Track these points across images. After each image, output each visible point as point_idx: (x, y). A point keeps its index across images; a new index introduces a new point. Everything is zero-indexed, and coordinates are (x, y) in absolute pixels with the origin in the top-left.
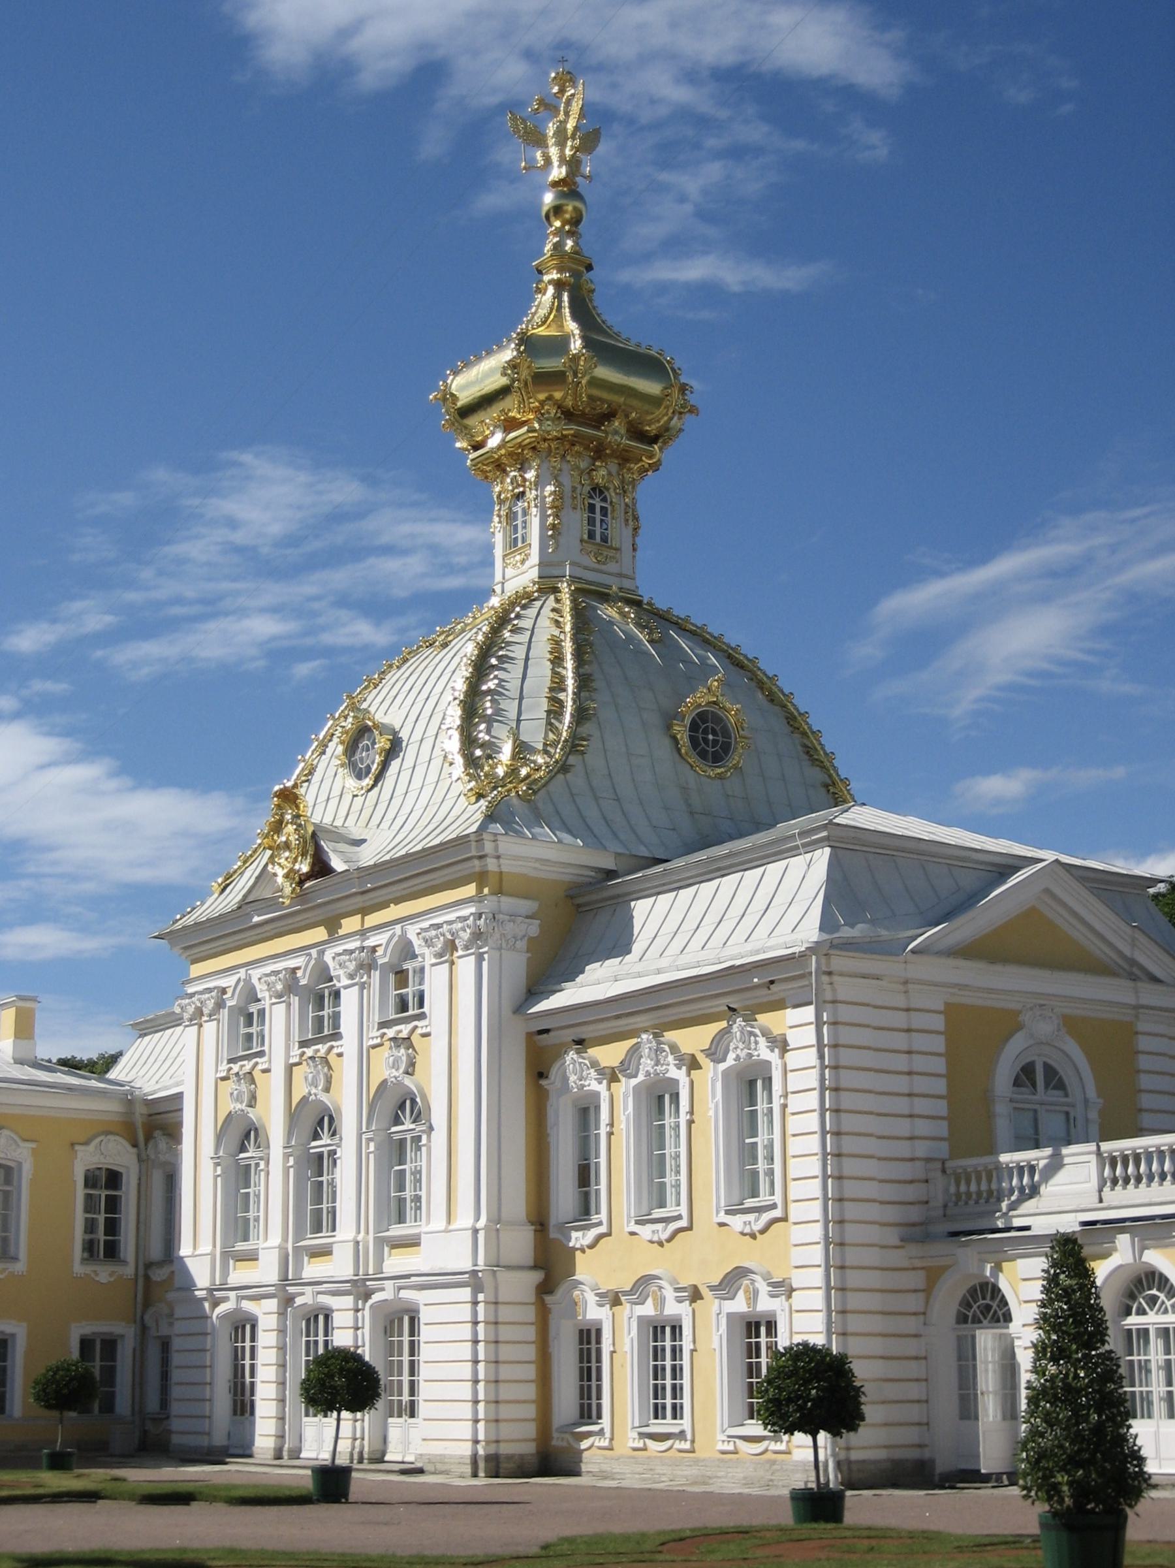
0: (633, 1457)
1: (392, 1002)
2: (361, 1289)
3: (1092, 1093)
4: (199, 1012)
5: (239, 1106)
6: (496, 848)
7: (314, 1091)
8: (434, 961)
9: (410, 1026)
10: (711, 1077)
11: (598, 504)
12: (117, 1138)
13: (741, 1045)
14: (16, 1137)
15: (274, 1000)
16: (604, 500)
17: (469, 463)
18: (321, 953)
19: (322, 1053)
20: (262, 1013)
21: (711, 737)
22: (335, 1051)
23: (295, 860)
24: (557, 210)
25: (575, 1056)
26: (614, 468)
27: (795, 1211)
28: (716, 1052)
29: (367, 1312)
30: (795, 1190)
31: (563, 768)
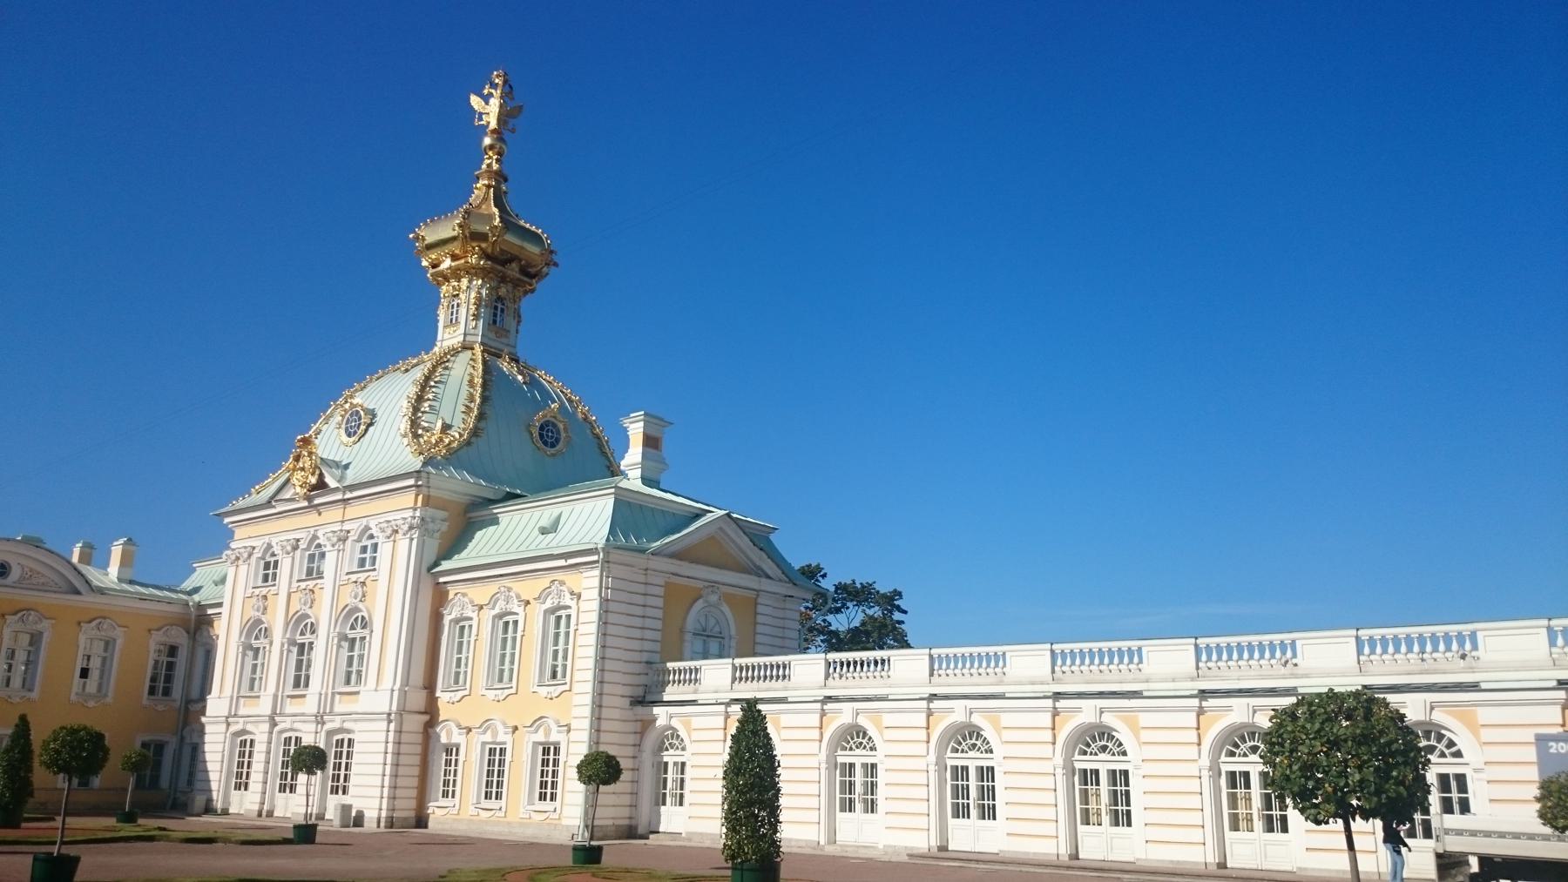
0: (471, 820)
1: (356, 562)
3: (733, 632)
4: (238, 558)
5: (257, 614)
6: (428, 482)
7: (304, 607)
10: (538, 610)
11: (500, 306)
15: (285, 555)
16: (503, 304)
17: (429, 275)
20: (276, 562)
21: (550, 434)
22: (319, 586)
23: (307, 478)
24: (491, 147)
25: (461, 598)
26: (510, 288)
27: (577, 688)
29: (323, 734)
30: (577, 676)
31: (468, 443)
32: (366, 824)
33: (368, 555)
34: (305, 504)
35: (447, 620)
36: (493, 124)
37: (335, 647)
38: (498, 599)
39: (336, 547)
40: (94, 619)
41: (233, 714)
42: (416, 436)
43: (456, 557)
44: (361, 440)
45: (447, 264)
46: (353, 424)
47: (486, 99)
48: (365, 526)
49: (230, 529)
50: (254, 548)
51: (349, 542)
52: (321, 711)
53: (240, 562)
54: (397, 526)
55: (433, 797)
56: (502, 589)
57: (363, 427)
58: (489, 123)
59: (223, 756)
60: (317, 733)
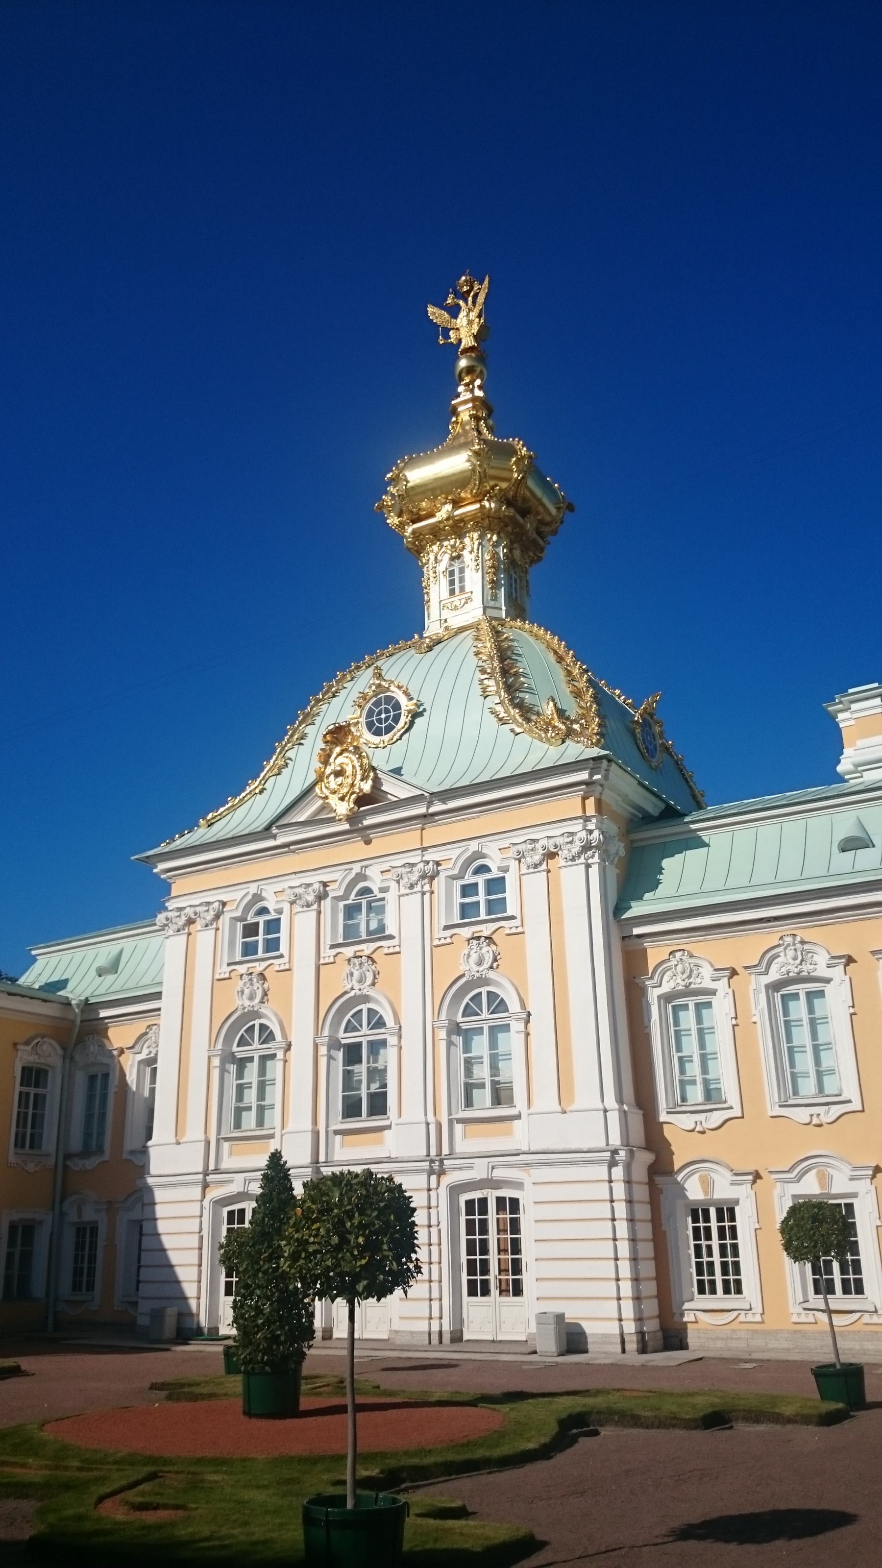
16: (515, 573)
19: (367, 952)
29: (443, 1192)
32: (590, 1347)
34: (346, 827)
35: (654, 994)
36: (468, 341)
37: (442, 1047)
38: (777, 956)
39: (418, 888)
41: (212, 1167)
43: (647, 896)
47: (454, 312)
48: (254, 895)
49: (164, 880)
50: (224, 904)
51: (440, 882)
53: (198, 925)
54: (556, 846)
55: (686, 1296)
56: (789, 940)
58: (460, 341)
59: (201, 1238)
60: (429, 1190)
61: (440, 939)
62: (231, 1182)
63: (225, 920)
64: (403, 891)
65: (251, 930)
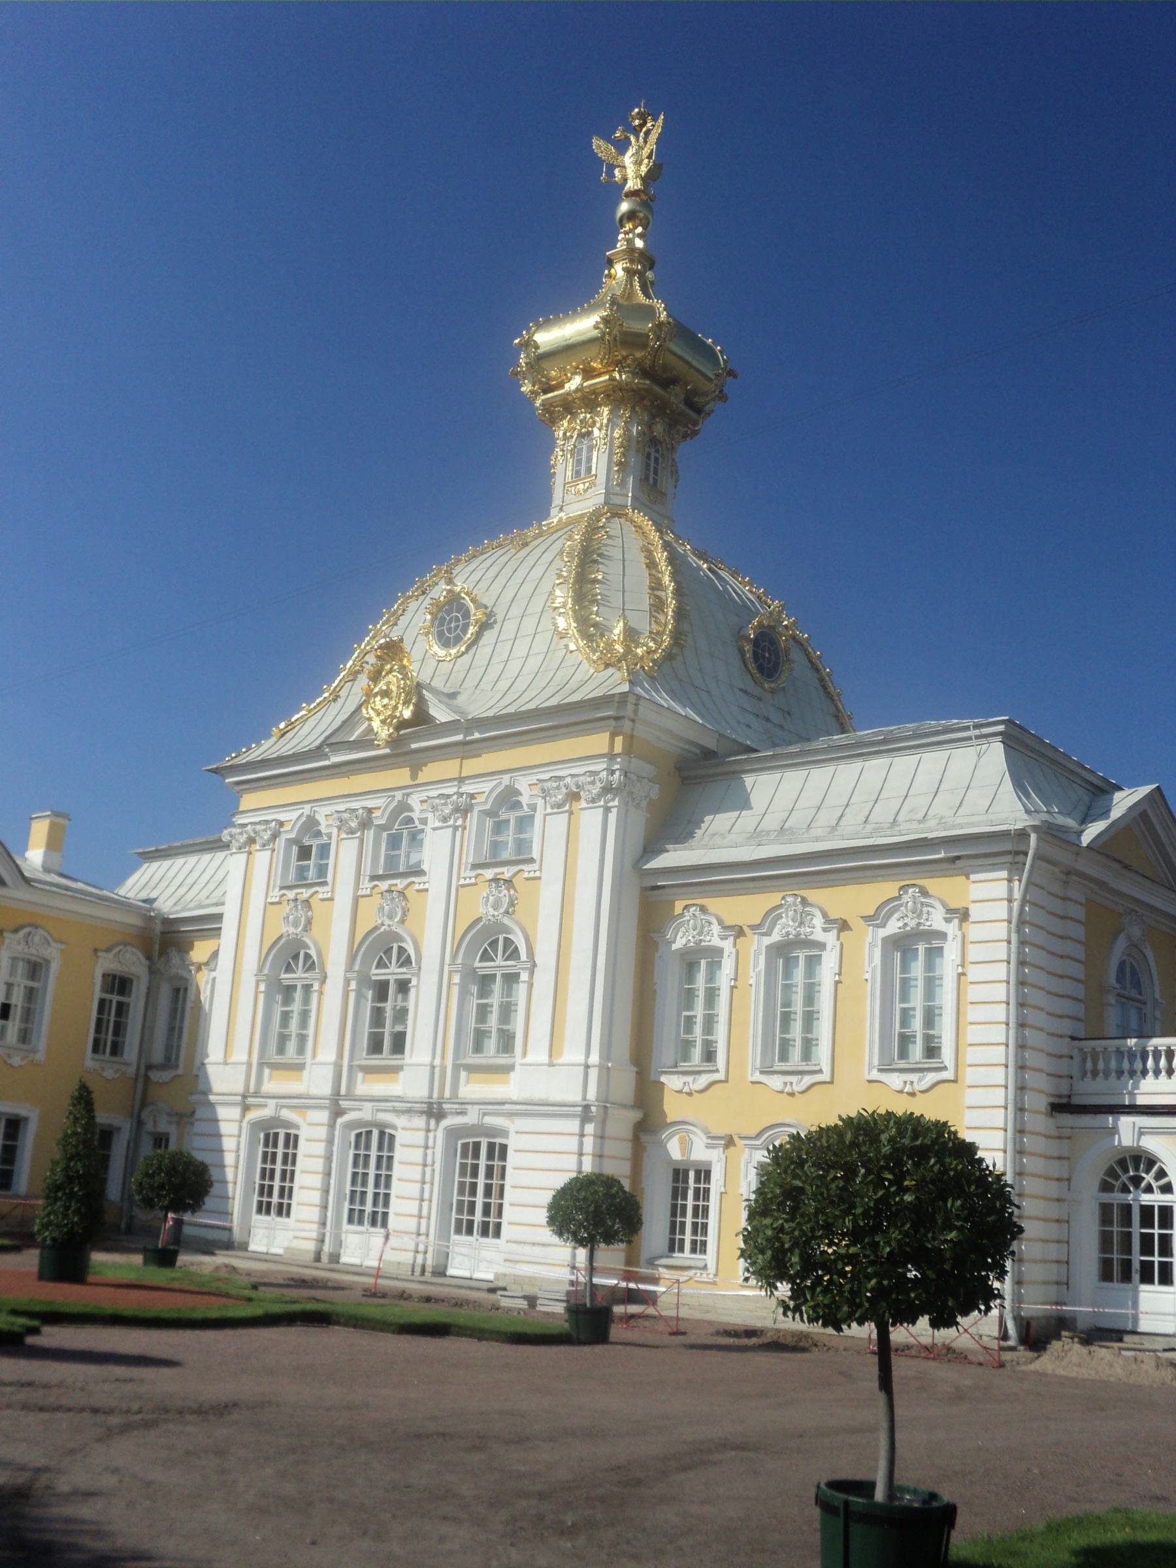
1: (486, 846)
2: (434, 1112)
6: (636, 711)
7: (387, 922)
8: (549, 810)
9: (514, 869)
12: (134, 950)
13: (910, 915)
14: (48, 937)
15: (344, 836)
16: (657, 451)
18: (408, 795)
19: (400, 887)
21: (767, 655)
23: (396, 708)
24: (631, 216)
25: (697, 913)
27: (970, 1076)
28: (875, 919)
29: (440, 1134)
33: (509, 836)
37: (455, 991)
38: (780, 917)
39: (451, 822)
40: (22, 927)
41: (252, 1089)
42: (589, 638)
44: (472, 652)
45: (575, 383)
46: (453, 625)
47: (622, 146)
52: (435, 1095)
54: (578, 786)
56: (790, 899)
57: (472, 630)
61: (465, 879)
62: (265, 1106)
63: (281, 843)
64: (438, 824)
65: (305, 853)
